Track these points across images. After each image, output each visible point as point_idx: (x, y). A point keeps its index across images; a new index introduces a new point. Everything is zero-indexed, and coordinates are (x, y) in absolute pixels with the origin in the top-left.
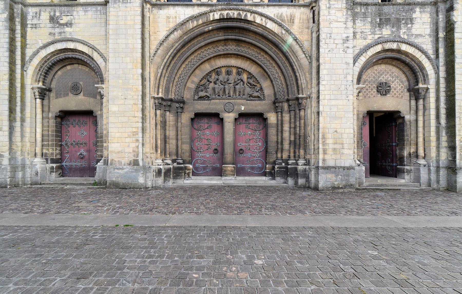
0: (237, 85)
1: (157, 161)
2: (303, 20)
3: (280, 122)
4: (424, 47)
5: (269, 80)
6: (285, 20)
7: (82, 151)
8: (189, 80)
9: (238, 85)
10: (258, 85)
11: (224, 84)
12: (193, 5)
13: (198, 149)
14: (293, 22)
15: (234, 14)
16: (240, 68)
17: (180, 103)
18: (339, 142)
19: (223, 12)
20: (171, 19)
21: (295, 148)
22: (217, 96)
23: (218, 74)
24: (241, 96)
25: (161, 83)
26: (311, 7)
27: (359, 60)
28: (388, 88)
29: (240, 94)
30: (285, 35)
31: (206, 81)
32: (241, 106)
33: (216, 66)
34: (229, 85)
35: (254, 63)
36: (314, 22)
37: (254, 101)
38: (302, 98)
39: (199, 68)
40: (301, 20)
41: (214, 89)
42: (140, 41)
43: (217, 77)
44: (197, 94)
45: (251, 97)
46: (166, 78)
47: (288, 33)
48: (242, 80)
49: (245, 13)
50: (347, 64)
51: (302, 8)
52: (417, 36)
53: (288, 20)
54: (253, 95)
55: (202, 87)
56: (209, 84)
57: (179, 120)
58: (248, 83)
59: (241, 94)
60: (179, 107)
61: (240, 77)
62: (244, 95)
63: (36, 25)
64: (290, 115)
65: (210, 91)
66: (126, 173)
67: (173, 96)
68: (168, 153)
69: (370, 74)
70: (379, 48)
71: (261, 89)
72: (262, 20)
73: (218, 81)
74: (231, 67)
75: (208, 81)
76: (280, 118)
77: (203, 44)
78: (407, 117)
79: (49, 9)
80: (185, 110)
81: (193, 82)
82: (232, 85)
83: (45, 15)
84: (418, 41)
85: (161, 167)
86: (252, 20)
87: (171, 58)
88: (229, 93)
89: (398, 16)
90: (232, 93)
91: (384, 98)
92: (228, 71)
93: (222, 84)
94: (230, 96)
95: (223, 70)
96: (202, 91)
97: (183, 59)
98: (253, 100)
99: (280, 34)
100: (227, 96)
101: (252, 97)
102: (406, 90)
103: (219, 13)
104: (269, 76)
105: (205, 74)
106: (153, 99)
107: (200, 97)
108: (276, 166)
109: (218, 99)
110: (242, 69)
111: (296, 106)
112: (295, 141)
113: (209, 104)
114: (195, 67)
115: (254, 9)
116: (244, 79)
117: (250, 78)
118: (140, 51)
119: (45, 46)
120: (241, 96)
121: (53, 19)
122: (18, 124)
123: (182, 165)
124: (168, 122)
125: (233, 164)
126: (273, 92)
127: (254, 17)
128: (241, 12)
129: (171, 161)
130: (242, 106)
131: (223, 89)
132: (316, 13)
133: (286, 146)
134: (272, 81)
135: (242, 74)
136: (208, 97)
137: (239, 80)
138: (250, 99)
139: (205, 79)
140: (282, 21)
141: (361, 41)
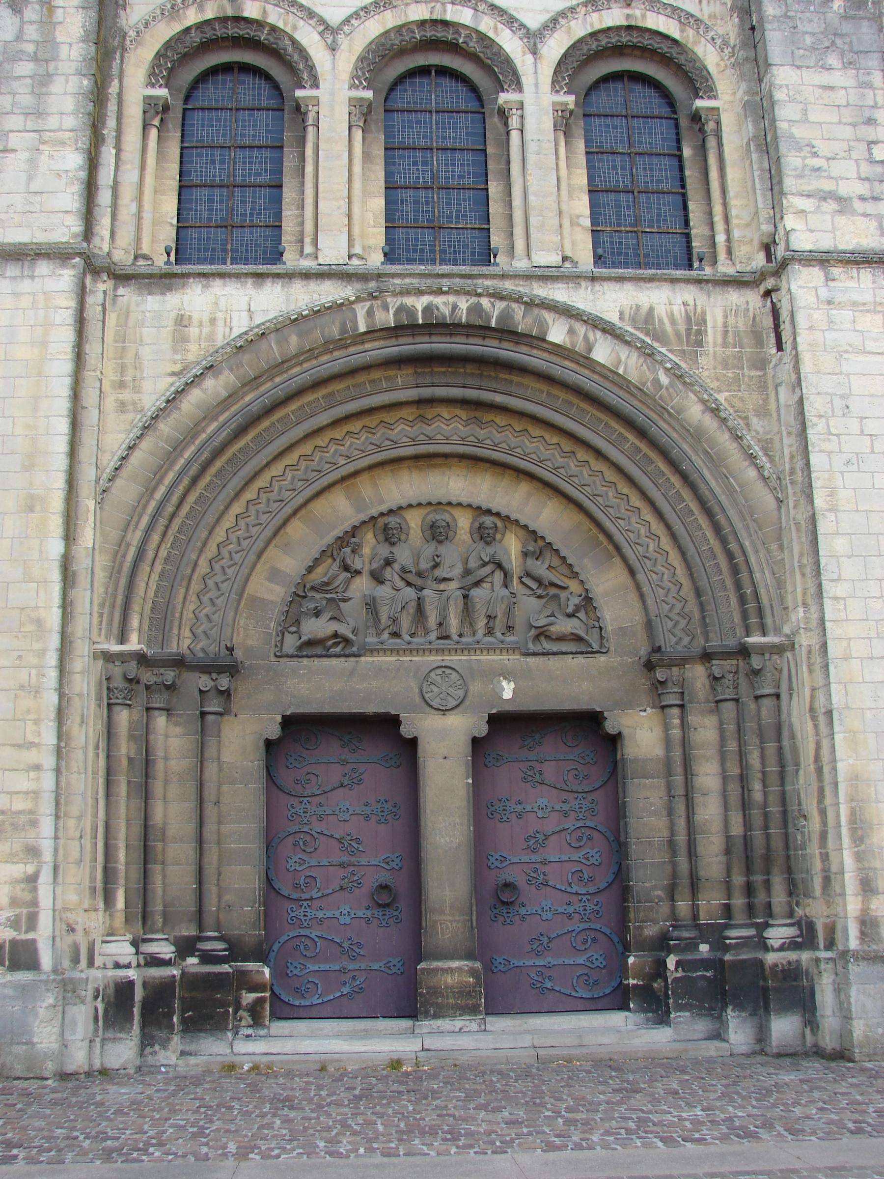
0: (477, 584)
2: (737, 334)
3: (677, 753)
5: (617, 560)
6: (664, 332)
8: (259, 566)
9: (484, 585)
10: (574, 586)
11: (419, 582)
12: (290, 276)
13: (296, 886)
14: (700, 344)
15: (455, 307)
16: (489, 512)
17: (219, 673)
19: (409, 301)
20: (191, 329)
21: (749, 870)
22: (386, 635)
23: (389, 536)
24: (499, 634)
26: (762, 289)
29: (491, 624)
30: (671, 390)
31: (335, 567)
32: (499, 682)
33: (382, 502)
34: (442, 586)
35: (551, 492)
36: (780, 347)
37: (556, 657)
38: (762, 650)
39: (303, 512)
40: (730, 334)
41: (371, 606)
42: (63, 426)
43: (384, 551)
44: (293, 629)
45: (542, 638)
46: (158, 567)
47: (685, 383)
48: (499, 566)
49: (500, 305)
53: (678, 335)
54: (552, 629)
55: (318, 596)
56: (348, 582)
57: (211, 751)
58: (528, 575)
59: (499, 625)
60: (213, 692)
61: (490, 550)
62: (510, 628)
64: (721, 723)
65: (353, 610)
67: (187, 642)
68: (160, 908)
71: (588, 601)
72: (571, 332)
73: (389, 569)
74: (448, 508)
75: (346, 568)
76: (676, 732)
77: (324, 419)
80: (237, 703)
81: (274, 575)
82: (453, 585)
87: (186, 481)
88: (441, 624)
90: (454, 624)
92: (433, 526)
93: (409, 584)
94: (447, 637)
95: (414, 520)
96: (317, 614)
97: (236, 482)
98: (554, 654)
99: (649, 387)
100: (433, 636)
101: (548, 637)
103: (394, 303)
104: (618, 548)
105: (330, 538)
106: (100, 662)
107: (310, 643)
108: (671, 962)
109: (392, 650)
110: (498, 514)
111: (743, 681)
112: (747, 840)
113: (351, 674)
114: (288, 510)
116: (509, 556)
117: (533, 553)
118: (61, 462)
120: (499, 634)
123: (226, 968)
125: (469, 956)
126: (638, 618)
128: (485, 302)
129: (173, 949)
130: (504, 683)
131: (413, 604)
132: (784, 315)
134: (632, 572)
135: (498, 536)
136: (347, 641)
137: (485, 564)
138: (538, 648)
139: (330, 561)
140: (656, 338)
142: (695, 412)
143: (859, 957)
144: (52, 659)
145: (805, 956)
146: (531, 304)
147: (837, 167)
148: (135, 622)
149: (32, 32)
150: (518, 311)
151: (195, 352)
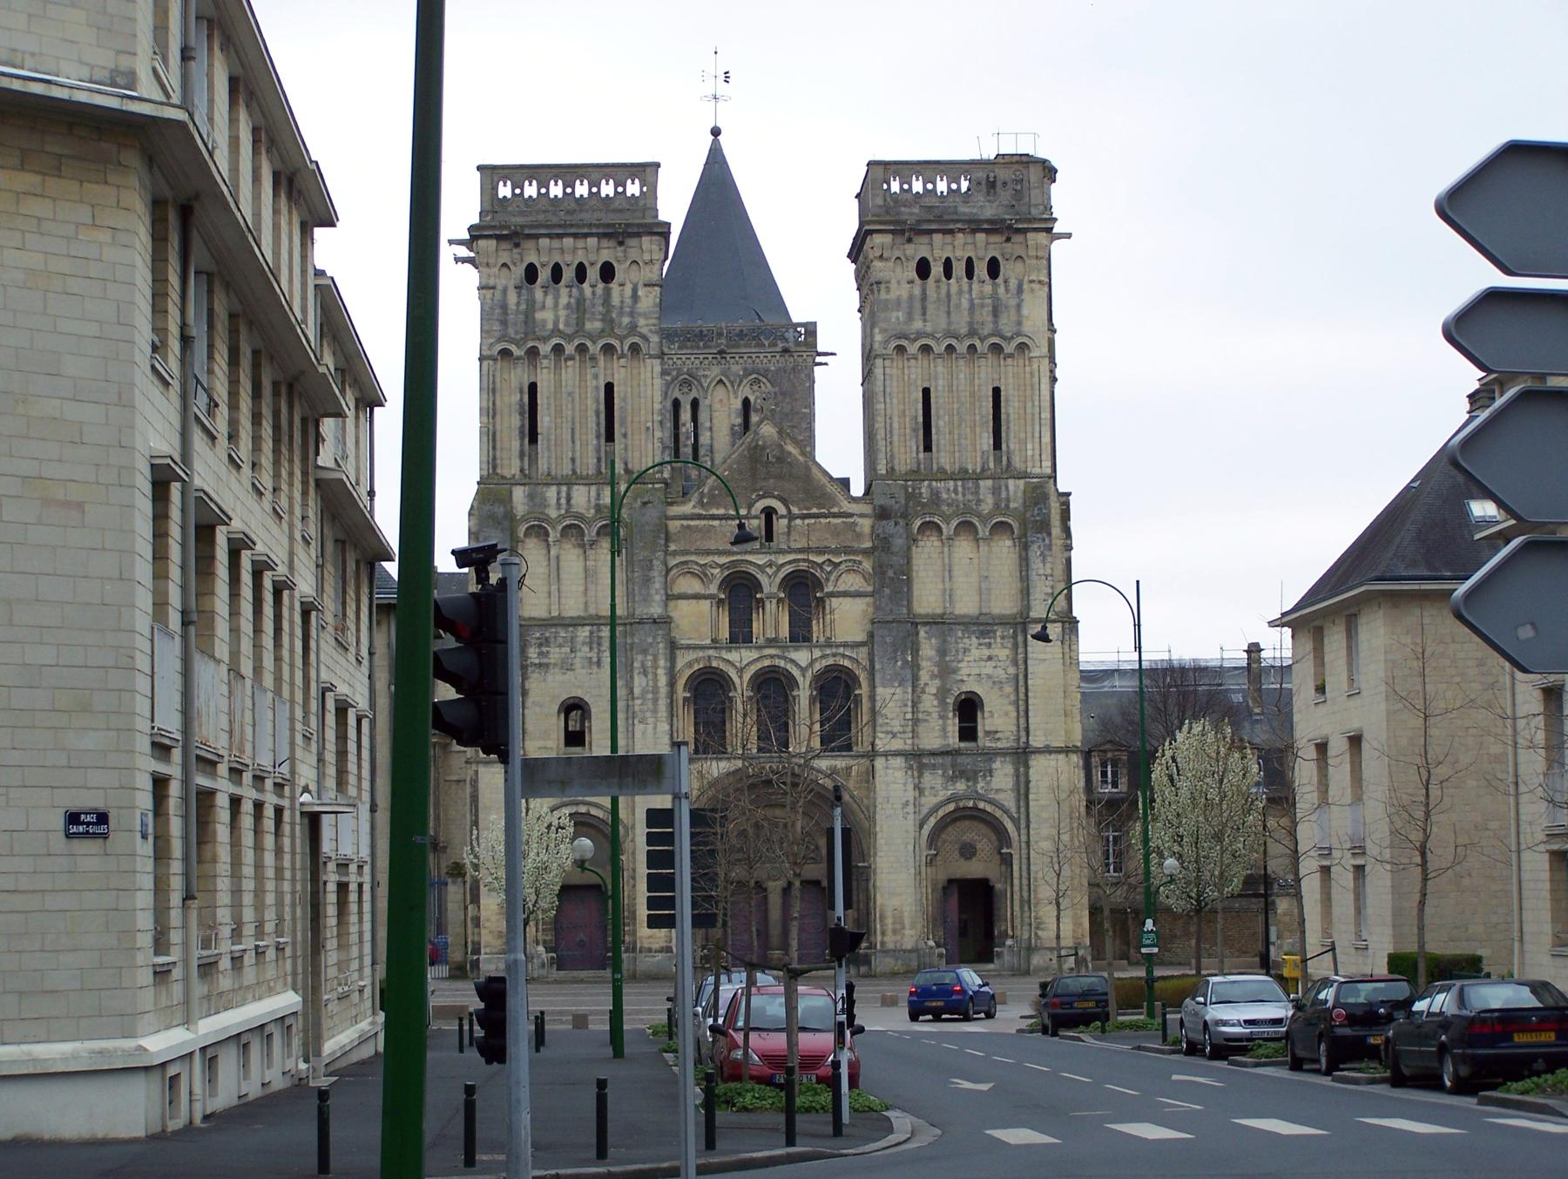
4: (1006, 804)
18: (899, 920)
50: (907, 831)
52: (998, 791)
66: (658, 961)
69: (951, 834)
70: (951, 807)
89: (974, 768)
91: (968, 863)
145: (869, 951)
149: (651, 683)
150: (796, 768)
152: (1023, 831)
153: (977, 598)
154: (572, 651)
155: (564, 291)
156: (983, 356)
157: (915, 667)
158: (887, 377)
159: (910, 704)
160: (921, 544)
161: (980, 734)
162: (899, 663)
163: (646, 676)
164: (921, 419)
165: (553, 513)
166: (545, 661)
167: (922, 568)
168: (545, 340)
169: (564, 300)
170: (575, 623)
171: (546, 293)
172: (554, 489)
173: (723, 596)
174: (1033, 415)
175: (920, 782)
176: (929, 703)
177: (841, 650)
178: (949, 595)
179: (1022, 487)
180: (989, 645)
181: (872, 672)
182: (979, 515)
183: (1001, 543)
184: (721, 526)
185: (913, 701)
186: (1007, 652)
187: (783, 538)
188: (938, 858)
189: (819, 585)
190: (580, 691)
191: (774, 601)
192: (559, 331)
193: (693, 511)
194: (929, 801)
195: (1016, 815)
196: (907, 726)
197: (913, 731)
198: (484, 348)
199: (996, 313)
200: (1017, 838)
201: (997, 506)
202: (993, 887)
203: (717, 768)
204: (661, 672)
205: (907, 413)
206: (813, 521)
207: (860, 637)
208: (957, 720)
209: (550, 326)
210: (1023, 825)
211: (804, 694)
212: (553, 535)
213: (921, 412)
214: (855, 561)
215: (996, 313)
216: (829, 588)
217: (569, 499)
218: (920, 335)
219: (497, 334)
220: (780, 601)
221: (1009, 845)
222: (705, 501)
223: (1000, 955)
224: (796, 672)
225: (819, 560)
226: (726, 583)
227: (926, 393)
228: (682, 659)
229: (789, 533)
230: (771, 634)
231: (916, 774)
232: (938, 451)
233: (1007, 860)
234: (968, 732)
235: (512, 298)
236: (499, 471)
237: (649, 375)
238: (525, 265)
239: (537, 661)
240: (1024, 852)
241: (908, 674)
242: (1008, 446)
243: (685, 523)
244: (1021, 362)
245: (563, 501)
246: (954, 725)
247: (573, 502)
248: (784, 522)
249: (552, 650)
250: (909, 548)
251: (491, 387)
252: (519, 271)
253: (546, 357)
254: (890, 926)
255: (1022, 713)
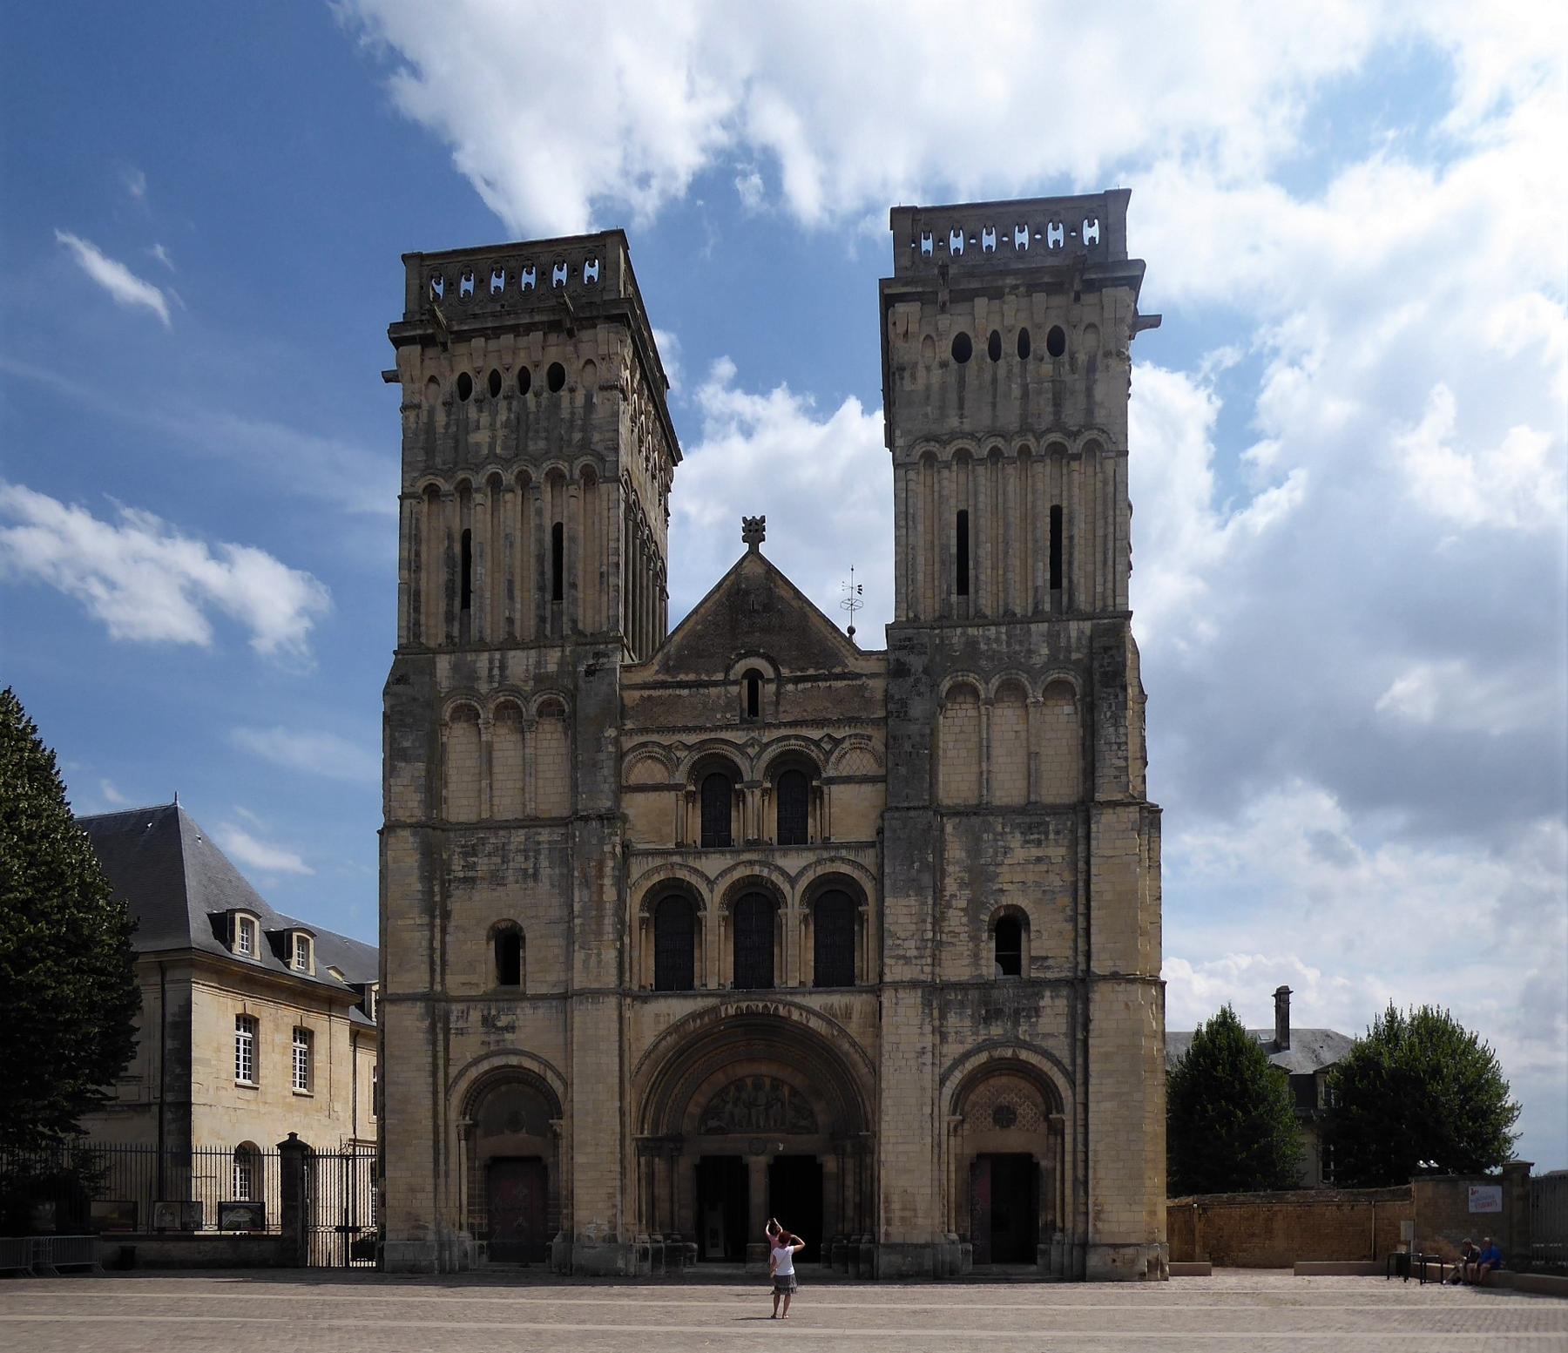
1: (641, 1236)
4: (1057, 1053)
7: (521, 1219)
25: (647, 1116)
27: (952, 1078)
28: (1011, 1116)
51: (864, 995)
52: (1047, 1036)
63: (462, 1029)
70: (983, 1057)
72: (801, 1015)
78: (1043, 1163)
79: (480, 1006)
83: (475, 1016)
84: (1049, 1044)
85: (648, 1245)
86: (786, 1014)
99: (830, 1037)
102: (1042, 1119)
115: (789, 998)
118: (617, 1074)
119: (476, 1061)
121: (487, 1021)
122: (442, 1180)
123: (681, 1244)
124: (657, 1174)
127: (789, 1011)
133: (850, 1212)
141: (955, 1046)
142: (846, 1046)
143: (885, 1246)
144: (618, 1142)
146: (786, 1004)
147: (907, 944)
148: (646, 1127)
149: (595, 898)
150: (781, 1008)
151: (663, 1027)
152: (1079, 1089)
153: (1025, 783)
154: (503, 862)
155: (503, 404)
156: (1041, 459)
157: (938, 872)
158: (910, 494)
159: (929, 920)
160: (949, 713)
161: (1024, 962)
162: (916, 865)
163: (589, 888)
164: (954, 550)
165: (484, 688)
166: (470, 874)
167: (951, 745)
168: (477, 468)
169: (502, 417)
170: (507, 826)
171: (480, 410)
172: (485, 656)
173: (693, 788)
174: (1105, 536)
175: (941, 1025)
176: (956, 920)
177: (844, 853)
178: (984, 780)
179: (1088, 632)
180: (1039, 843)
181: (879, 880)
182: (1029, 670)
183: (1057, 710)
184: (690, 695)
185: (934, 917)
186: (1062, 851)
187: (770, 710)
188: (966, 1126)
189: (816, 770)
190: (512, 911)
191: (758, 792)
192: (495, 455)
193: (656, 678)
194: (953, 1050)
195: (1070, 1068)
196: (926, 948)
197: (934, 957)
198: (407, 484)
199: (1057, 403)
200: (1071, 1099)
201: (1053, 658)
202: (1038, 1164)
203: (677, 1008)
204: (608, 881)
205: (936, 542)
206: (809, 685)
207: (866, 834)
208: (993, 945)
209: (485, 451)
210: (1079, 1077)
211: (793, 913)
212: (486, 714)
213: (954, 541)
214: (862, 737)
215: (1057, 403)
216: (830, 772)
217: (503, 667)
218: (954, 435)
219: (421, 465)
220: (765, 792)
221: (1061, 1110)
222: (671, 663)
223: (1046, 1253)
224: (786, 888)
225: (816, 734)
226: (695, 770)
227: (963, 517)
228: (637, 868)
229: (777, 703)
230: (752, 835)
231: (936, 1013)
232: (977, 592)
233: (1056, 1130)
234: (1009, 958)
235: (441, 418)
236: (423, 640)
237: (605, 504)
238: (456, 376)
239: (461, 875)
240: (1080, 1116)
241: (926, 879)
242: (1070, 581)
243: (646, 693)
244: (1090, 470)
245: (496, 672)
246: (989, 950)
247: (508, 672)
248: (772, 687)
249: (480, 861)
250: (934, 716)
251: (413, 532)
252: (449, 383)
253: (478, 490)
254: (898, 1214)
255: (1081, 932)
